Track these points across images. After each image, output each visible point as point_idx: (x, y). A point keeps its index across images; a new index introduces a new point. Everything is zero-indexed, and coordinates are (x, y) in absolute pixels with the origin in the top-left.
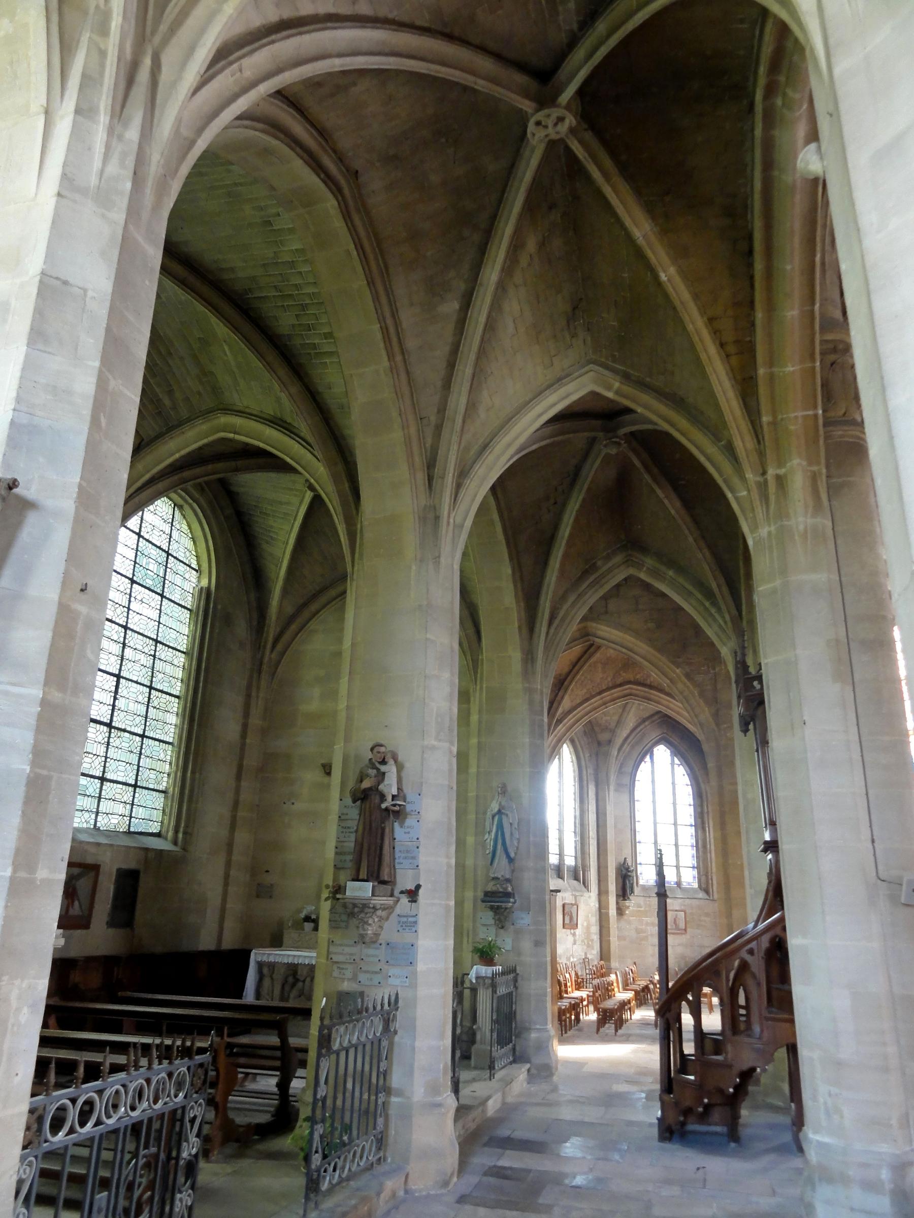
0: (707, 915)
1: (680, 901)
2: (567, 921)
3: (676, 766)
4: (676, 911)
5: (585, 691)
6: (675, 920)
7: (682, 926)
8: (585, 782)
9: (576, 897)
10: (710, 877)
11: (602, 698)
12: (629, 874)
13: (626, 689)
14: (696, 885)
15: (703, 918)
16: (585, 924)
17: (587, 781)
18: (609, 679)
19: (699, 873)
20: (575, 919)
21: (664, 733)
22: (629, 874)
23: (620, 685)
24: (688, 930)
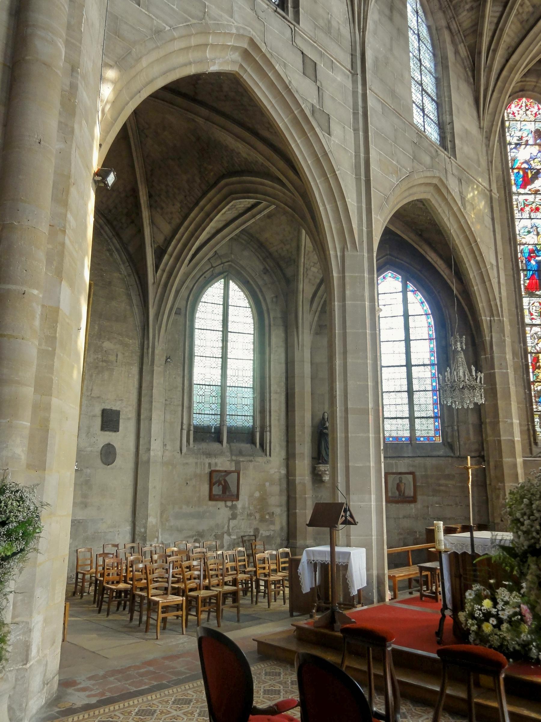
0: (448, 477)
1: (407, 461)
2: (217, 490)
3: (410, 295)
4: (400, 473)
5: (178, 205)
6: (398, 486)
7: (409, 492)
8: (267, 329)
9: (237, 463)
10: (456, 428)
11: (202, 209)
12: (325, 431)
13: (223, 188)
14: (439, 440)
15: (442, 482)
16: (257, 494)
17: (270, 325)
18: (198, 180)
19: (443, 423)
20: (234, 489)
21: (387, 255)
22: (325, 431)
23: (216, 183)
24: (419, 498)
